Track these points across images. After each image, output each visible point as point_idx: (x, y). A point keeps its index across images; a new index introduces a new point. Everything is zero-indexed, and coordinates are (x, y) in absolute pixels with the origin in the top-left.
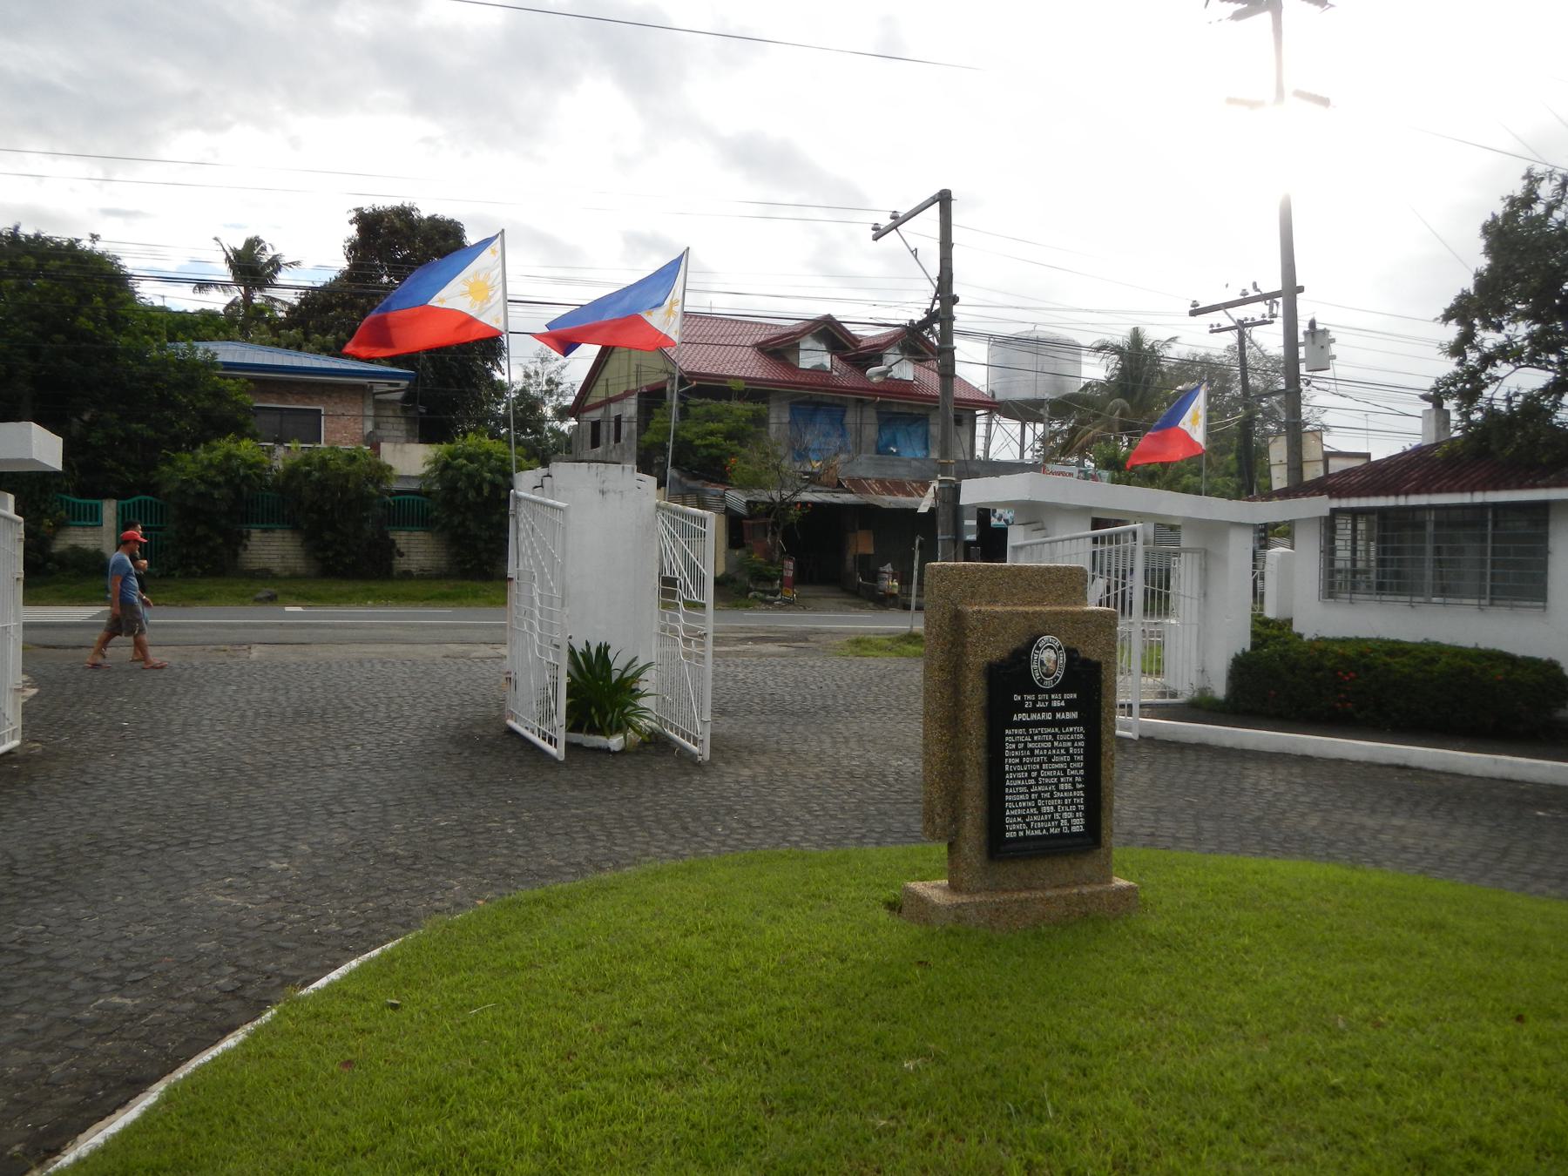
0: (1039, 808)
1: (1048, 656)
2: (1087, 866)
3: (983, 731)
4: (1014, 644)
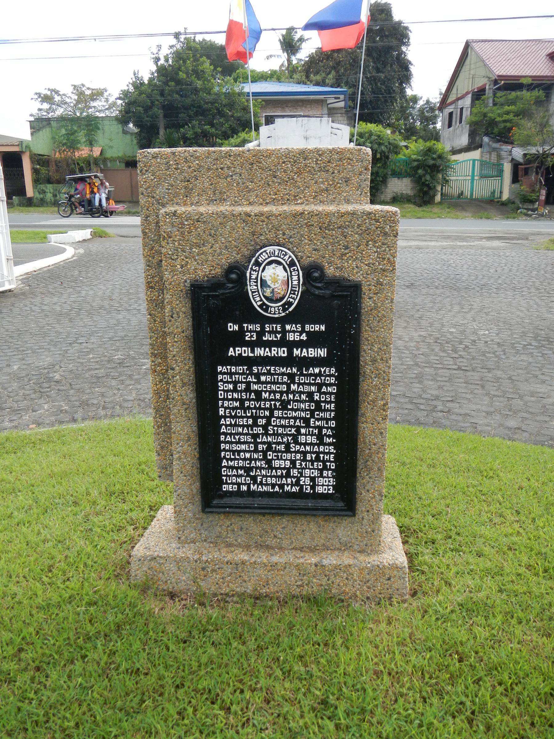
0: (269, 462)
2: (343, 529)
3: (190, 365)
4: (227, 258)
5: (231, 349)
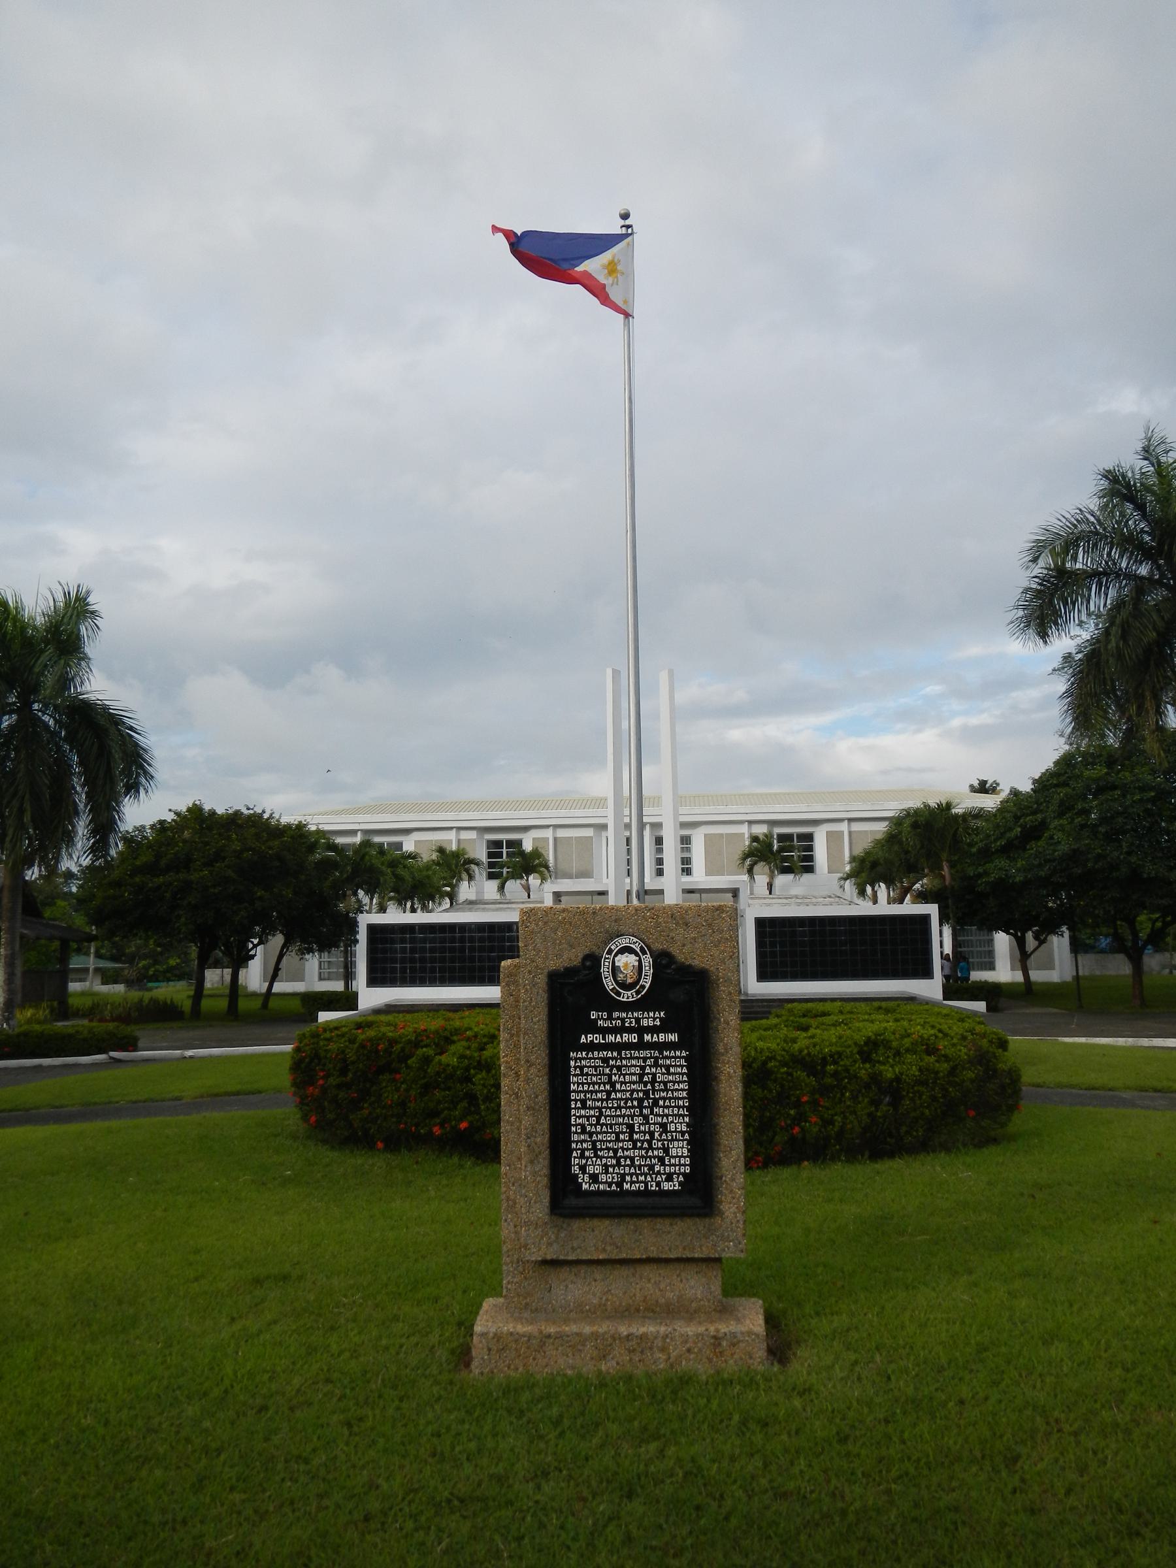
1: (626, 962)
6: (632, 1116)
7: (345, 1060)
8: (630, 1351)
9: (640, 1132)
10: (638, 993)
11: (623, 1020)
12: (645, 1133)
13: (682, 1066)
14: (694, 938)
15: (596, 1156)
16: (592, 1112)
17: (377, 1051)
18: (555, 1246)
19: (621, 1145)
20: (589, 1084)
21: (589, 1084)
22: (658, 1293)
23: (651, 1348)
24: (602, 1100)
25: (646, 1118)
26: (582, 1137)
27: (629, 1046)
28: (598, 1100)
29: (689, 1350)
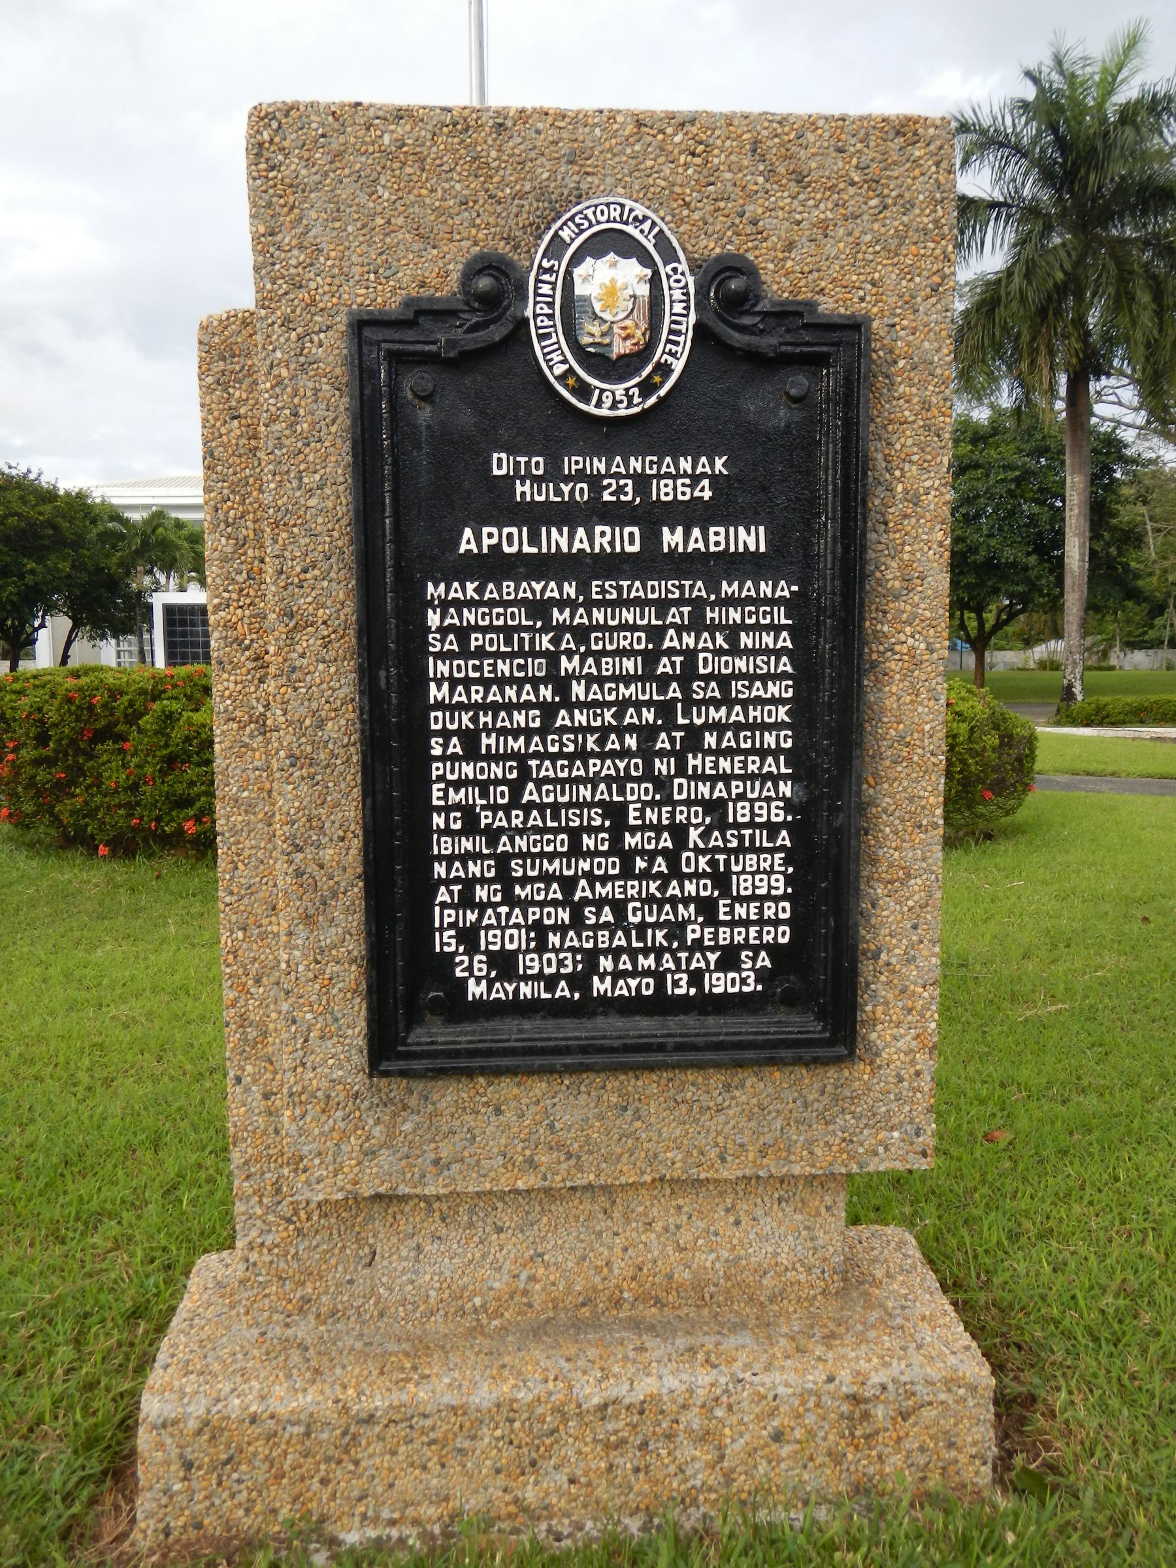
5: (468, 533)
6: (621, 781)
7: (42, 722)
8: (608, 1446)
9: (643, 828)
10: (647, 388)
11: (595, 483)
12: (658, 829)
13: (777, 629)
14: (824, 226)
15: (510, 900)
16: (497, 770)
17: (91, 708)
18: (384, 1156)
19: (585, 865)
20: (486, 683)
21: (486, 683)
22: (674, 1256)
23: (670, 1437)
24: (528, 733)
25: (662, 784)
26: (467, 844)
27: (611, 565)
28: (516, 733)
29: (778, 1437)
